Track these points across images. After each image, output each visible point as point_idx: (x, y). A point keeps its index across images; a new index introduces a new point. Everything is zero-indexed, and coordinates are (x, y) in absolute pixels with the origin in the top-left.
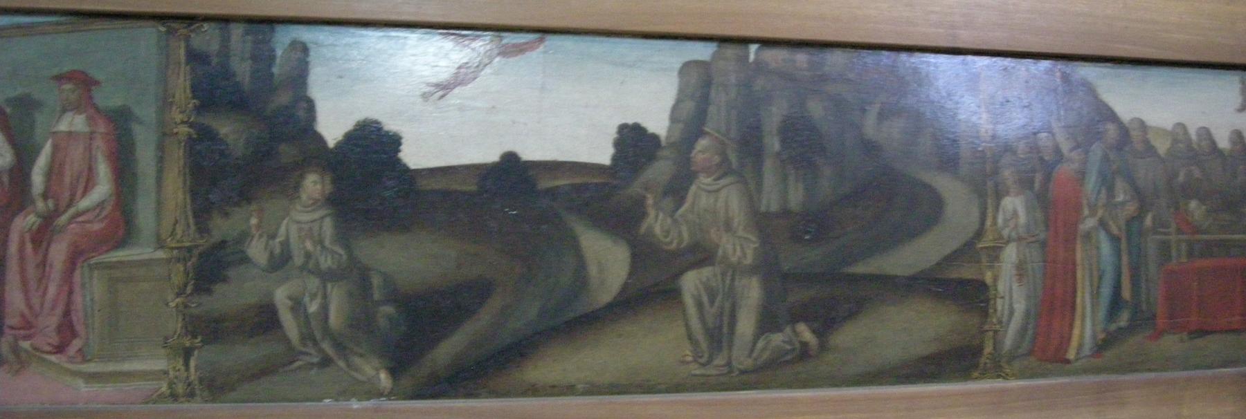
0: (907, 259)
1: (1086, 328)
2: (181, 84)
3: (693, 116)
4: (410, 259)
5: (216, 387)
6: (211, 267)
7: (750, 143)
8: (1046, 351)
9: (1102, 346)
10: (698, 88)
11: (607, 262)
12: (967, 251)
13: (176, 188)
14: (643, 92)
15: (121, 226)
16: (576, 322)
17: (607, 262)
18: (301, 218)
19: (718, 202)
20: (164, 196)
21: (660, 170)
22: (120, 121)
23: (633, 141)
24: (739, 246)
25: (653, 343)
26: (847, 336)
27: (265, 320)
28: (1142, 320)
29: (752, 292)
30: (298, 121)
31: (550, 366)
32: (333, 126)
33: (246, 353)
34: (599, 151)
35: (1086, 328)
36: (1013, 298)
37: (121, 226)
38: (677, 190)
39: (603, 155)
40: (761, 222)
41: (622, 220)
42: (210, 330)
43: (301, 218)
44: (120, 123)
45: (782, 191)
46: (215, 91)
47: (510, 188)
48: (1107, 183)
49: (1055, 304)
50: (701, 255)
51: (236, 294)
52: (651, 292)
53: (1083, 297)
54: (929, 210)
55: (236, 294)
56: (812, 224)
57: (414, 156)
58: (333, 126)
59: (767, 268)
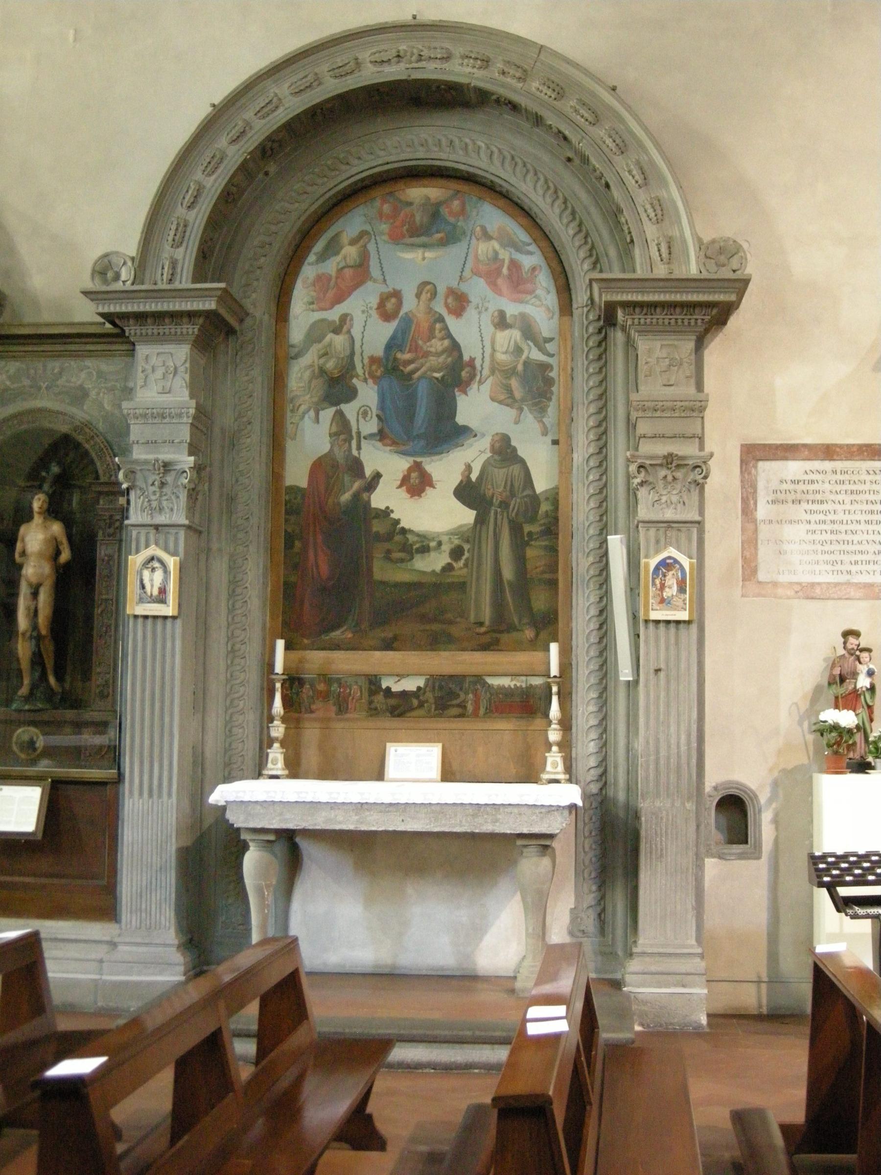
0: (455, 702)
1: (482, 711)
2: (367, 682)
3: (426, 685)
4: (392, 702)
5: (371, 716)
6: (371, 702)
7: (434, 687)
8: (475, 714)
9: (485, 714)
10: (427, 681)
11: (415, 702)
12: (464, 701)
13: (367, 694)
14: (421, 682)
15: (361, 698)
16: (412, 709)
17: (415, 702)
18: (380, 697)
19: (429, 696)
20: (366, 694)
21: (422, 691)
22: (361, 687)
23: (419, 688)
24: (432, 700)
25: (421, 712)
26: (446, 712)
27: (376, 709)
28: (491, 711)
29: (433, 706)
30: (380, 686)
31: (408, 715)
32: (384, 687)
33: (374, 712)
34: (415, 689)
35: (482, 711)
36: (470, 707)
37: (361, 698)
38: (424, 693)
39: (415, 689)
40: (435, 697)
41: (418, 697)
42: (370, 709)
43: (380, 697)
44: (361, 687)
45: (438, 694)
46: (371, 682)
47: (404, 694)
48: (486, 692)
49: (477, 708)
50: (427, 701)
51: (373, 706)
52: (421, 705)
53: (481, 708)
54: (458, 695)
55: (373, 706)
56: (442, 698)
57: (393, 690)
58: (384, 687)
59: (435, 703)
